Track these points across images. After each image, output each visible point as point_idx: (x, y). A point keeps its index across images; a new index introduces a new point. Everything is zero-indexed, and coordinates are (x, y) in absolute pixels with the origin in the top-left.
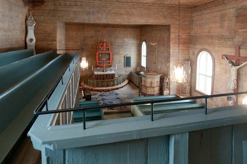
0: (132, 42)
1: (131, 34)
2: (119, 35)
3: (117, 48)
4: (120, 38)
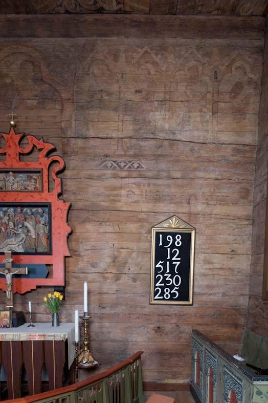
0: (198, 135)
1: (193, 80)
2: (115, 88)
3: (99, 178)
4: (116, 109)
